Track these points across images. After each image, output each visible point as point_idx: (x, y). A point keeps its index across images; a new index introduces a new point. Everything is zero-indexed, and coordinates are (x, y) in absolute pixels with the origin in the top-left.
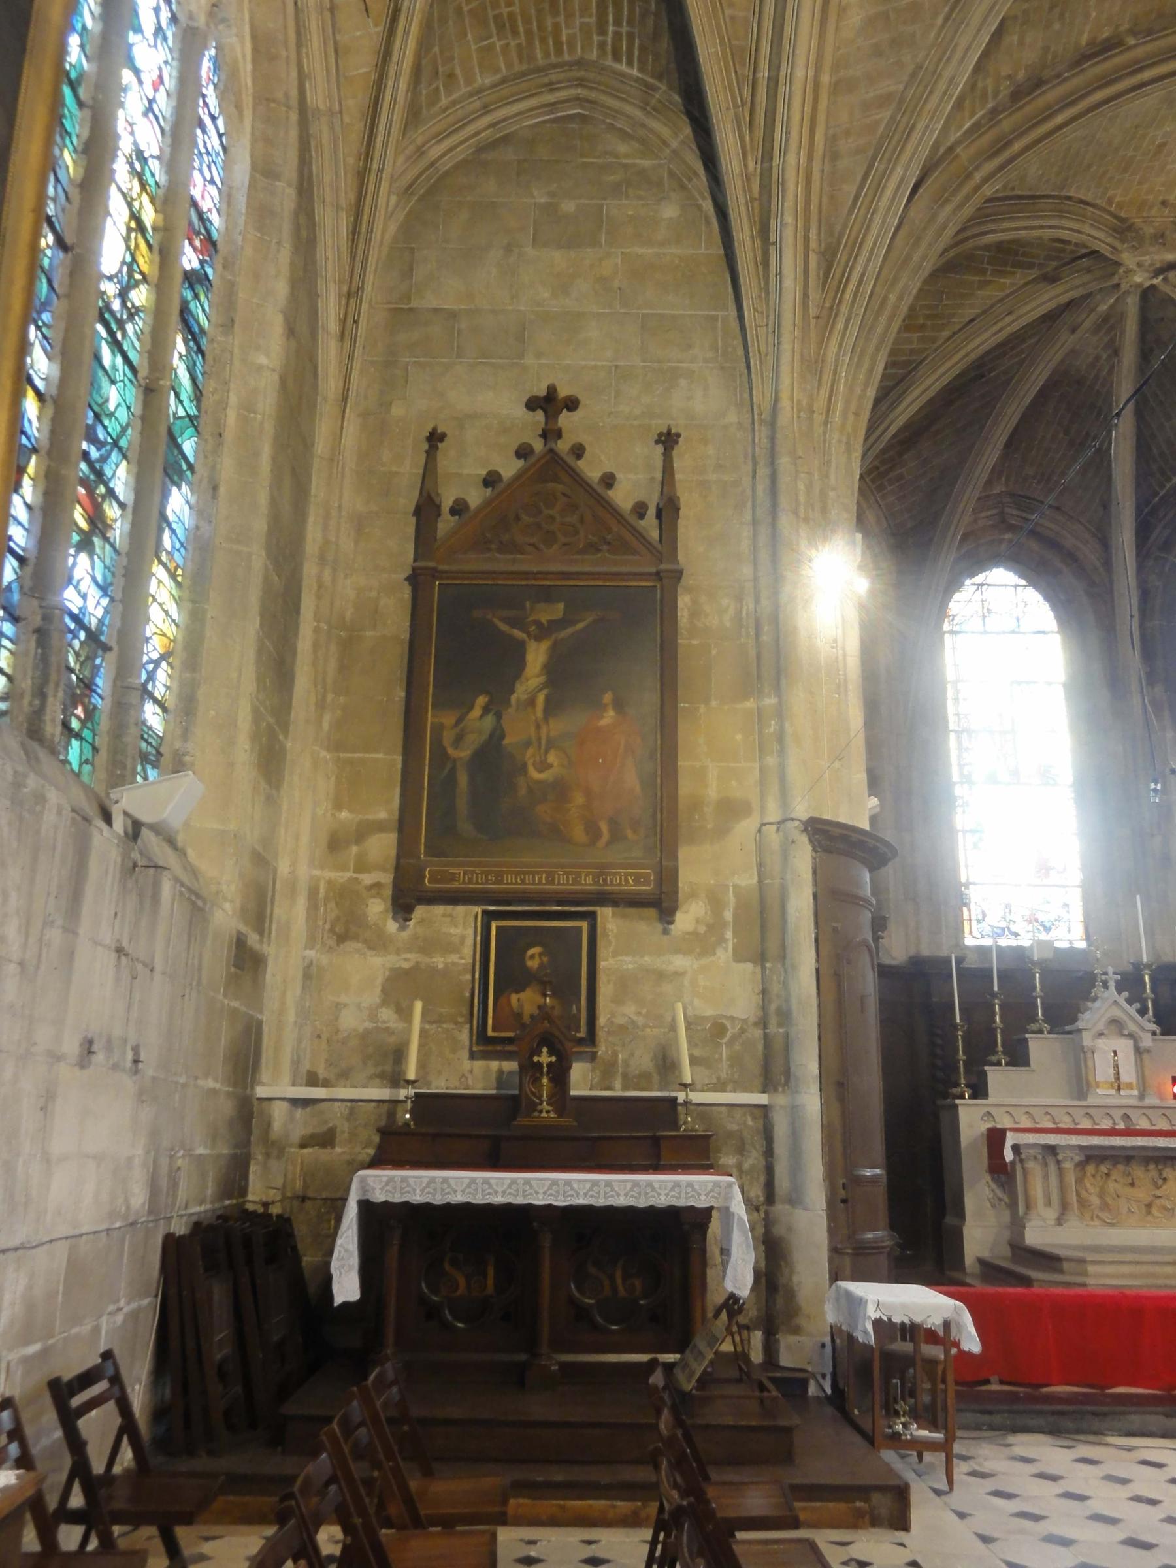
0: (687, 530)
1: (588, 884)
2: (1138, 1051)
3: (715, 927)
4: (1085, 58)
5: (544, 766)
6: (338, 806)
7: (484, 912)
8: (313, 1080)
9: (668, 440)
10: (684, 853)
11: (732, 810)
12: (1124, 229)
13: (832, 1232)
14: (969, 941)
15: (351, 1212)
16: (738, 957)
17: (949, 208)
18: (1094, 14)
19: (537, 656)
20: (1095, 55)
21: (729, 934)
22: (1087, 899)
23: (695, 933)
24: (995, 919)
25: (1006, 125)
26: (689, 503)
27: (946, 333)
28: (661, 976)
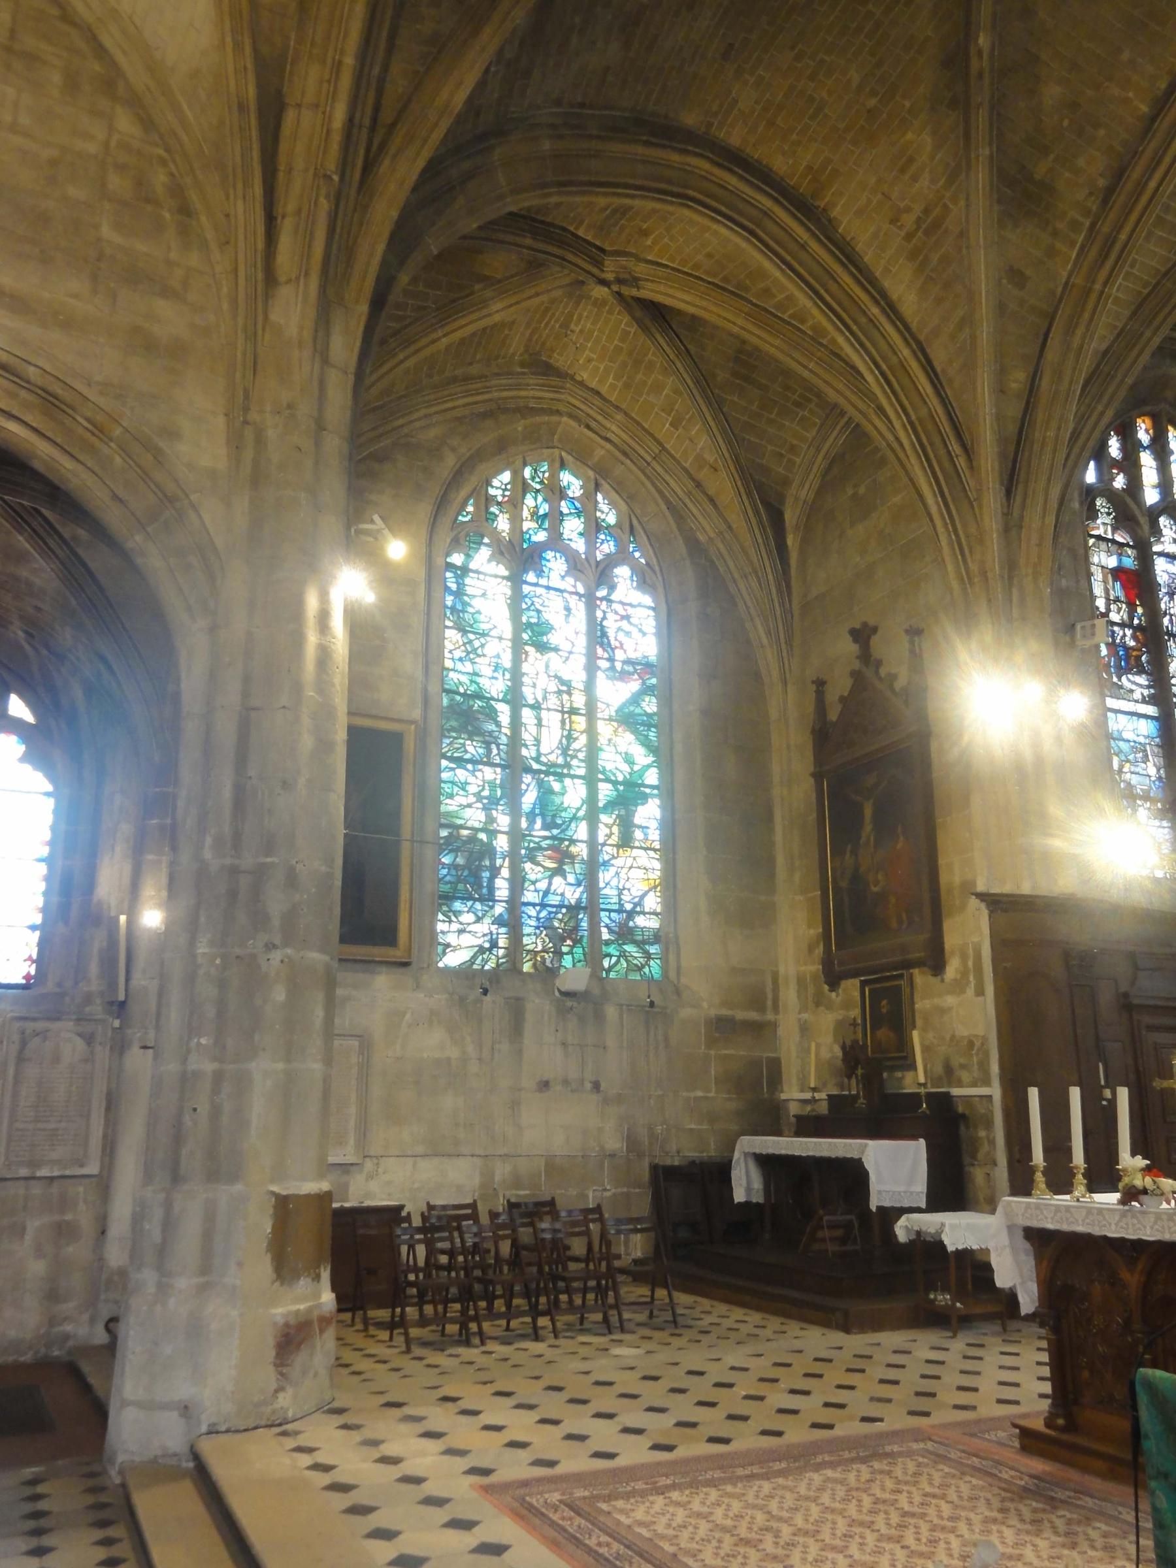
1: (898, 958)
3: (964, 973)
4: (1153, 119)
5: (876, 883)
7: (861, 982)
10: (947, 925)
17: (1079, 332)
18: (1131, 94)
19: (868, 811)
20: (1161, 110)
23: (955, 980)
25: (1106, 229)
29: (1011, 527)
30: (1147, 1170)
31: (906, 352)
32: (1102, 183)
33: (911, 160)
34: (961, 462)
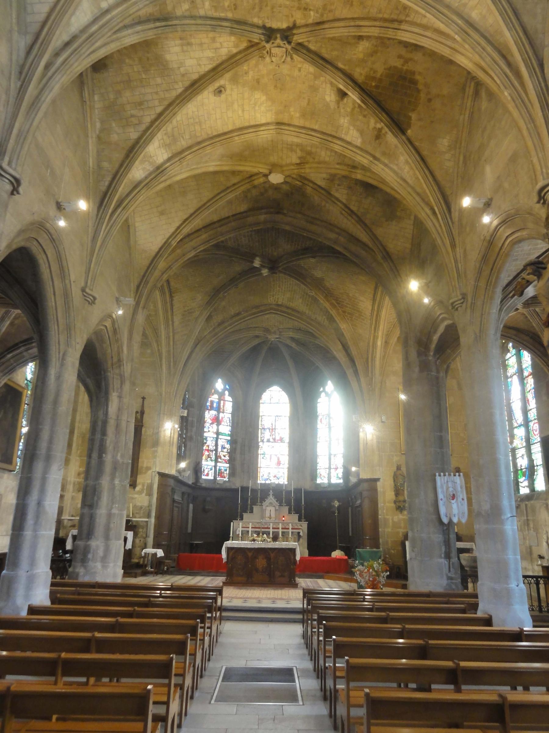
0: (145, 416)
2: (276, 510)
6: (80, 467)
8: (72, 516)
9: (144, 398)
11: (148, 468)
12: (267, 330)
13: (154, 542)
14: (259, 482)
15: (70, 536)
16: (146, 495)
21: (145, 491)
22: (289, 471)
23: (139, 491)
24: (266, 477)
26: (146, 410)
27: (238, 346)
28: (133, 498)
29: (179, 384)
30: (257, 537)
31: (171, 334)
32: (220, 321)
33: (195, 299)
34: (172, 364)
